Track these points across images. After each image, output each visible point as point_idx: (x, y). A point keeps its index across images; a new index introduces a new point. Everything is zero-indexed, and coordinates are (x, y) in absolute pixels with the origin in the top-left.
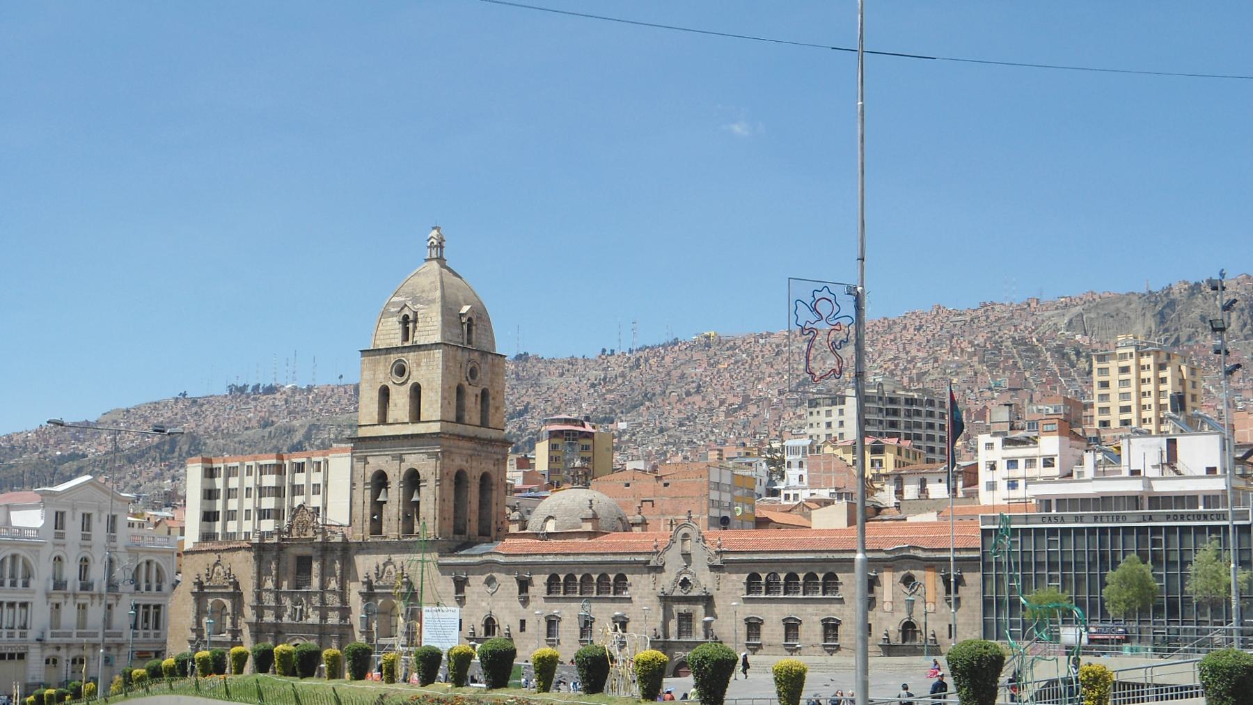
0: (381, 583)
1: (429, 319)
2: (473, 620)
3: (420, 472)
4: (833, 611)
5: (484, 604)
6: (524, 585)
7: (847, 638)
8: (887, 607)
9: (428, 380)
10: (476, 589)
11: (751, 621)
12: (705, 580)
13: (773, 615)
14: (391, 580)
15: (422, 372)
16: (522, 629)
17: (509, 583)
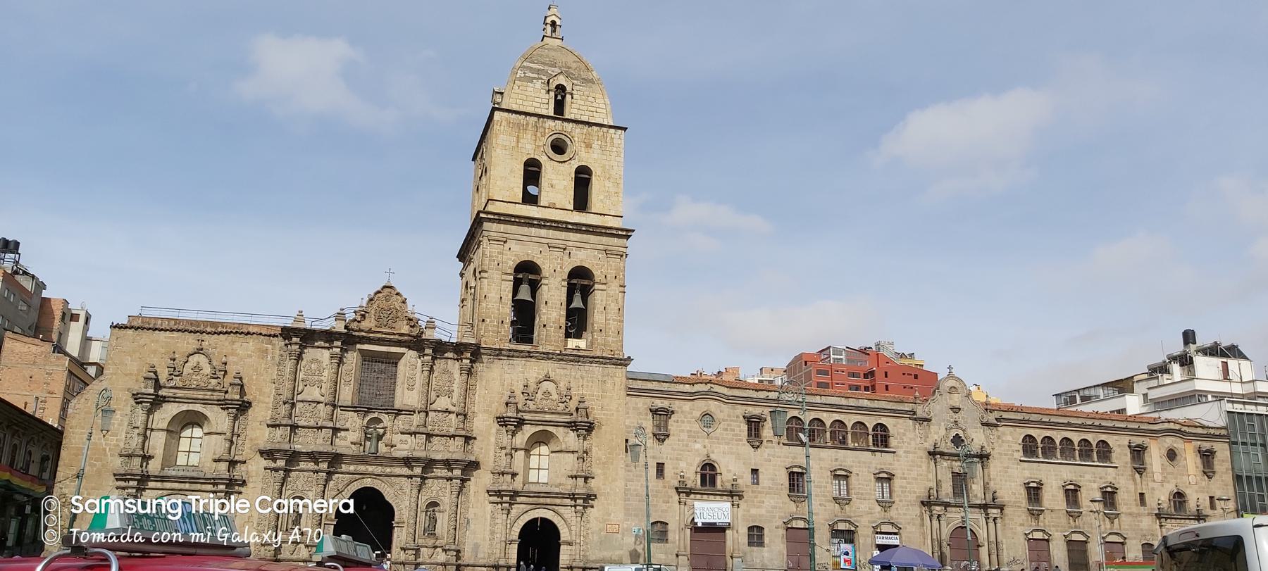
0: (532, 406)
1: (590, 99)
2: (683, 465)
3: (597, 273)
4: (1108, 476)
5: (698, 446)
6: (754, 425)
7: (1125, 507)
8: (1158, 477)
9: (604, 166)
10: (686, 427)
11: (1032, 485)
12: (978, 438)
13: (1054, 476)
14: (546, 405)
15: (595, 156)
16: (756, 482)
17: (731, 419)
